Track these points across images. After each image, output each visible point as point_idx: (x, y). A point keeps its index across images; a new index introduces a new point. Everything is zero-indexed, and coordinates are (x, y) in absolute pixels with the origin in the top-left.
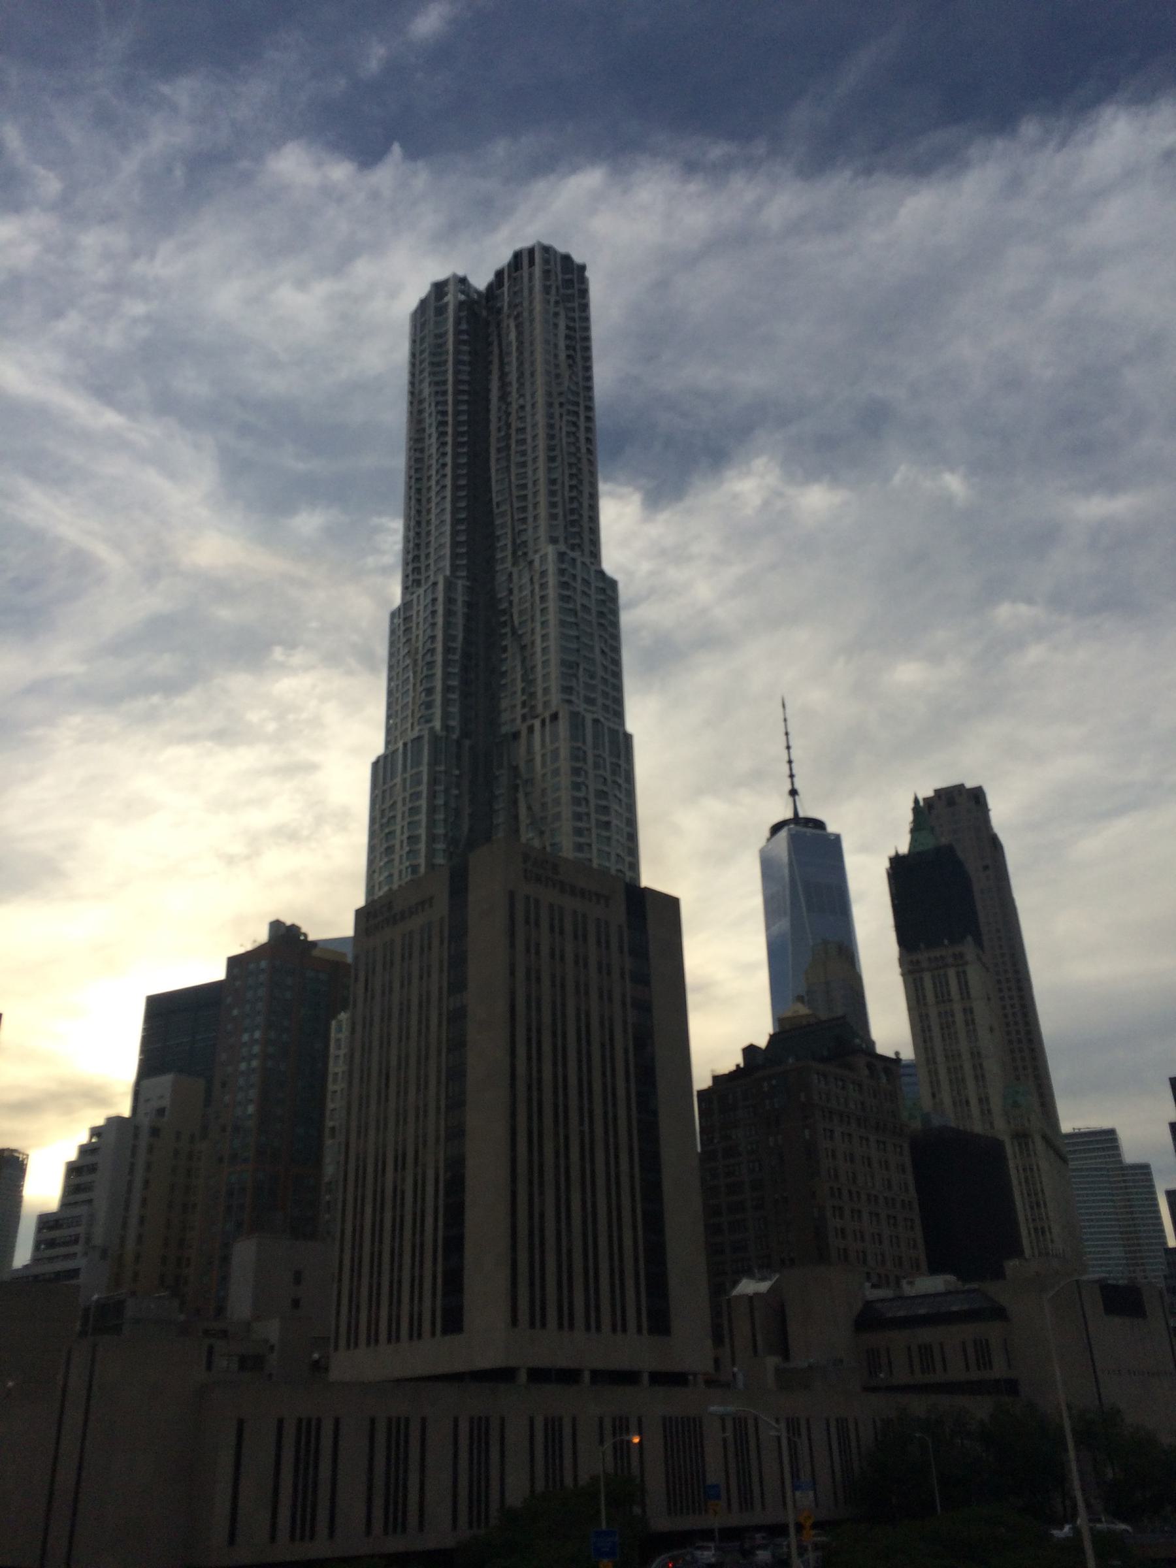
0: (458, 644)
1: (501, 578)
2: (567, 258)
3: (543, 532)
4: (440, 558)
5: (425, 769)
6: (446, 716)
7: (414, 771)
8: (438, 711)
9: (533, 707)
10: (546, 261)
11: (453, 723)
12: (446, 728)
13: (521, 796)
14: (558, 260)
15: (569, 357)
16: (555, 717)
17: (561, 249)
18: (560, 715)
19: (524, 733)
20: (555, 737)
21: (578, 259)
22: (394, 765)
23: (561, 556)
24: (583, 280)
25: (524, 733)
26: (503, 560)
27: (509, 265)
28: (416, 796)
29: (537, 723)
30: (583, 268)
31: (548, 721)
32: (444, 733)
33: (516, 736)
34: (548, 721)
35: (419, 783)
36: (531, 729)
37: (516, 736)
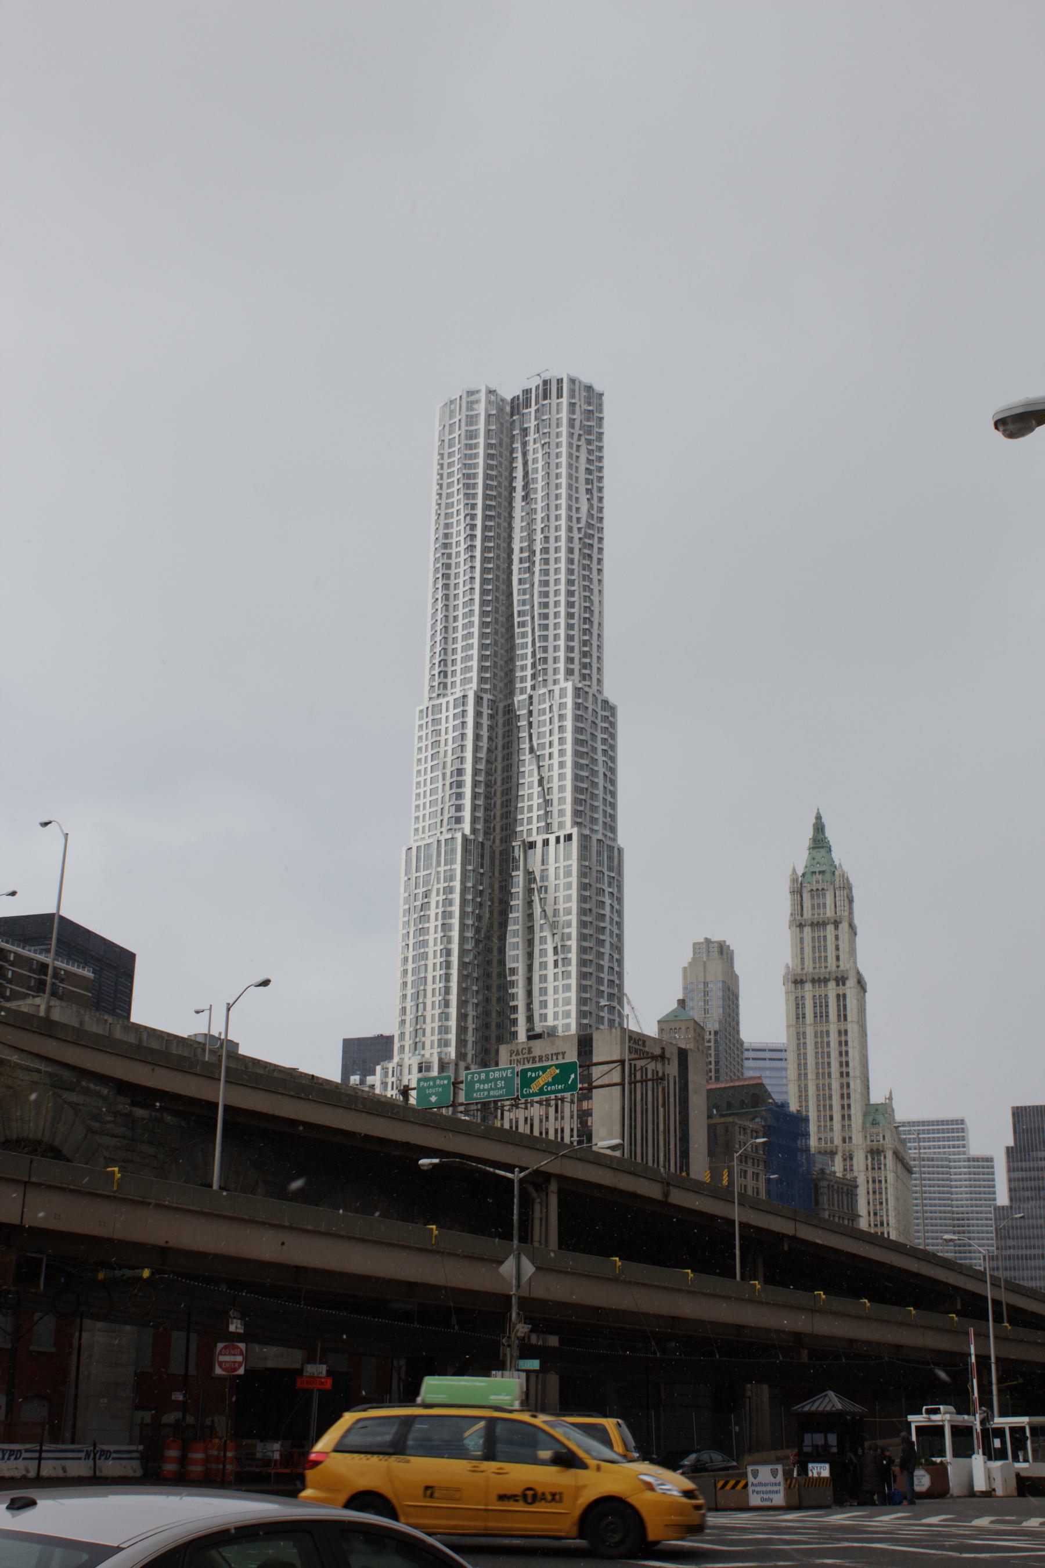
0: (483, 755)
1: (519, 698)
2: (589, 388)
3: (561, 665)
4: (467, 669)
5: (458, 867)
6: (474, 820)
7: (448, 867)
8: (467, 814)
9: (548, 825)
10: (572, 394)
11: (479, 827)
12: (474, 831)
13: (536, 898)
14: (582, 388)
15: (587, 490)
16: (569, 837)
17: (586, 380)
18: (575, 837)
19: (539, 845)
20: (568, 857)
21: (598, 388)
22: (428, 857)
23: (577, 691)
24: (600, 407)
25: (539, 845)
26: (523, 679)
27: (537, 387)
28: (449, 890)
29: (552, 838)
30: (601, 395)
31: (562, 839)
32: (472, 837)
33: (532, 845)
34: (562, 839)
35: (452, 878)
36: (546, 843)
37: (532, 845)
